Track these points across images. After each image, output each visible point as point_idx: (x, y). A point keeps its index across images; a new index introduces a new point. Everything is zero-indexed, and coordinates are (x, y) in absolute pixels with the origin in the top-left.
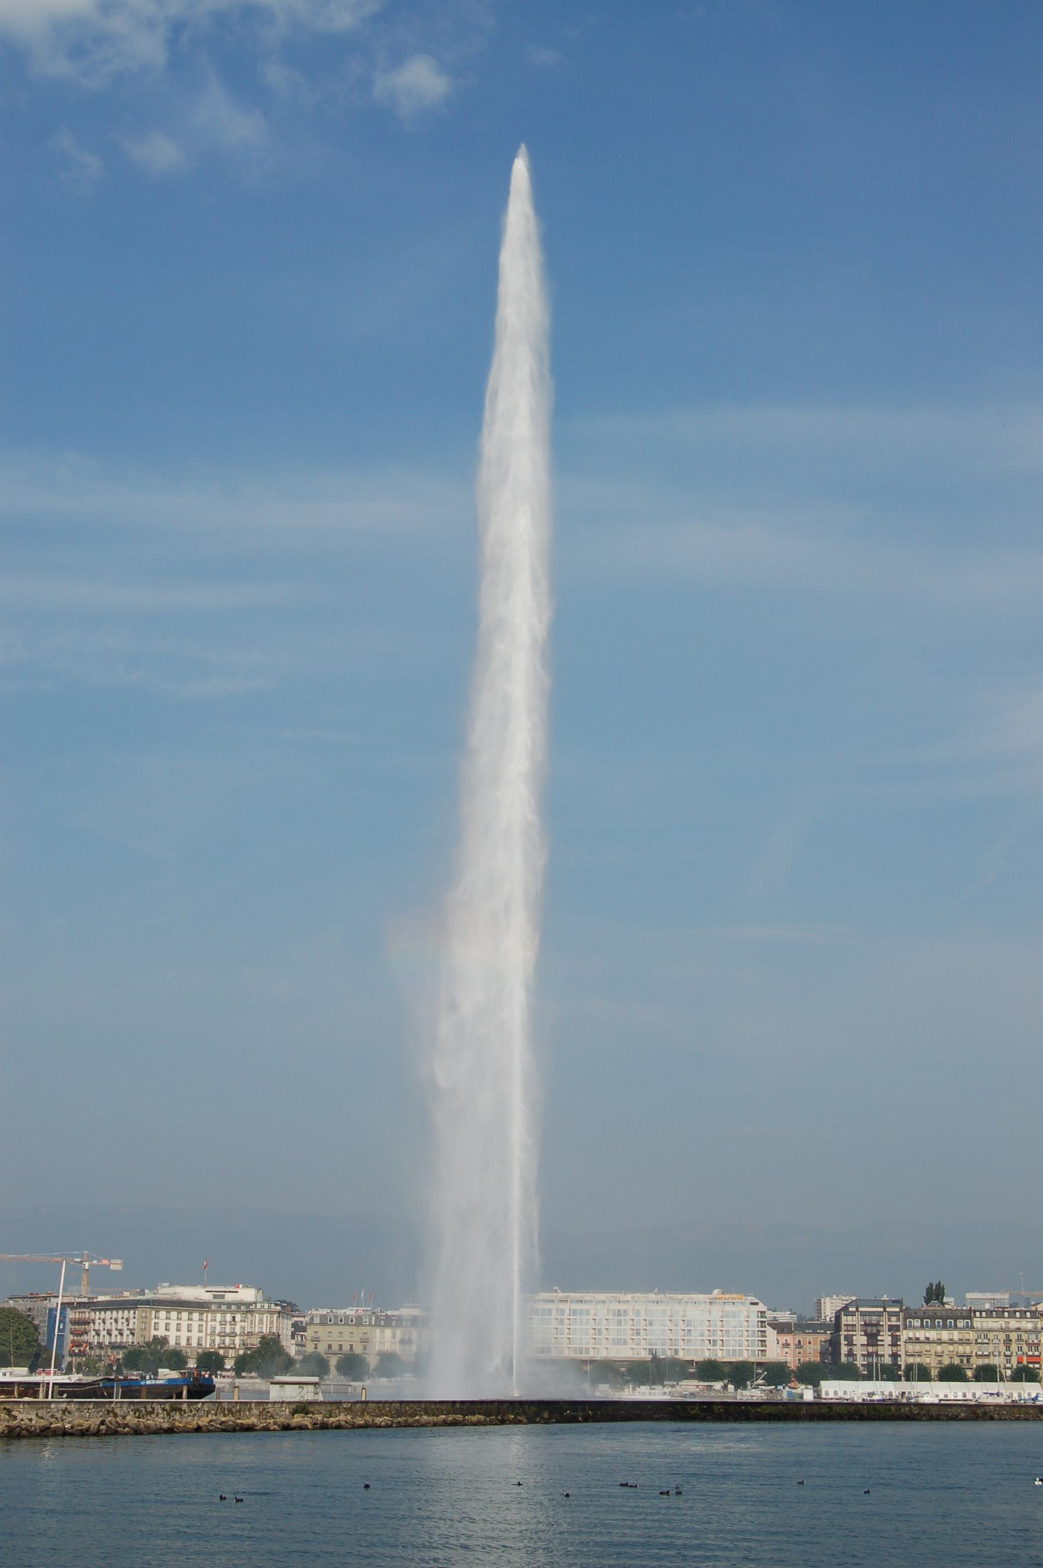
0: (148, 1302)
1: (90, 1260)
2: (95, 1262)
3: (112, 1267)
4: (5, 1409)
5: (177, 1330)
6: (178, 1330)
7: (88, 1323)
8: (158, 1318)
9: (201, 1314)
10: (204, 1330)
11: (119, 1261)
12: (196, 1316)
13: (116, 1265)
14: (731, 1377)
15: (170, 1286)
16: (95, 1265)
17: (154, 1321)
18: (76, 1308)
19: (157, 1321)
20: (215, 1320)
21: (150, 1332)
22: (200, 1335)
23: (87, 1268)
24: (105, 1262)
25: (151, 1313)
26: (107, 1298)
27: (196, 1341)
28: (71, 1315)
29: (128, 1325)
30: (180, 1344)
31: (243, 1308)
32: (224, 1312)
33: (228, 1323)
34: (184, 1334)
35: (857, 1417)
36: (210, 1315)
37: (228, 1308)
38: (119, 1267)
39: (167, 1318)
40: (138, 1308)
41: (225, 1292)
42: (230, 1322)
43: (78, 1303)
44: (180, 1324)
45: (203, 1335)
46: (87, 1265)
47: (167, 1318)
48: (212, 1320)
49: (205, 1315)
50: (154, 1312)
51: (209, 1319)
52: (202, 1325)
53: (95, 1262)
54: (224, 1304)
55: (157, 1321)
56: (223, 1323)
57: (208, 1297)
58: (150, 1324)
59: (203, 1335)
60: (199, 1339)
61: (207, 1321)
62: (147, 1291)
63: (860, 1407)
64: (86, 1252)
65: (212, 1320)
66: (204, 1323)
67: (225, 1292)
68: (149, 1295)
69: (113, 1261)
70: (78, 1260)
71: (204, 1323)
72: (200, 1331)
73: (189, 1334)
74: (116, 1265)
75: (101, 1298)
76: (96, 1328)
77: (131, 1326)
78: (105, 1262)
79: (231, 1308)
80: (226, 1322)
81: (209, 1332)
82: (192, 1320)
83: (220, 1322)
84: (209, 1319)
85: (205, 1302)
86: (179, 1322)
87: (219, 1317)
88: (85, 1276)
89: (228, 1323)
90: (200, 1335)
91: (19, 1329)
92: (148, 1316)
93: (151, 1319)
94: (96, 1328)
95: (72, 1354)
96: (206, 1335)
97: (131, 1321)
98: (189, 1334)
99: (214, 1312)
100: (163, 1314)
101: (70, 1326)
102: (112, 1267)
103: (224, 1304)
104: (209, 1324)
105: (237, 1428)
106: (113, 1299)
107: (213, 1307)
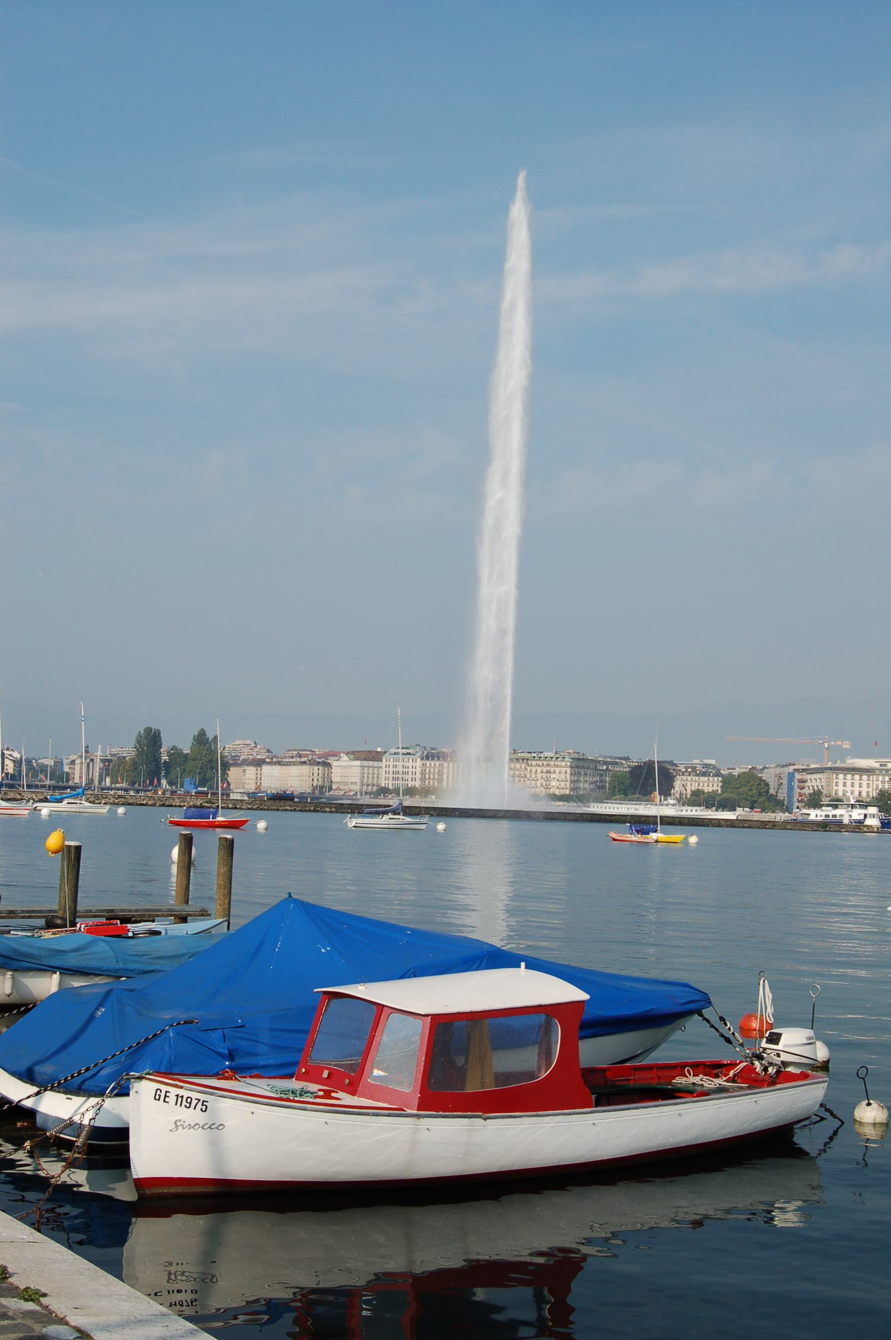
0: (831, 769)
1: (829, 741)
2: (832, 743)
3: (844, 746)
4: (18, 793)
5: (860, 787)
6: (844, 786)
7: (805, 782)
8: (838, 779)
9: (869, 776)
10: (871, 785)
11: (848, 742)
12: (865, 777)
13: (846, 745)
14: (721, 806)
15: (851, 758)
16: (832, 744)
17: (835, 781)
18: (801, 772)
19: (837, 780)
20: (878, 780)
21: (832, 787)
22: (868, 790)
23: (826, 747)
24: (839, 743)
25: (833, 776)
26: (818, 766)
27: (858, 794)
28: (798, 776)
29: (821, 783)
30: (838, 795)
31: (884, 772)
32: (884, 775)
33: (886, 782)
34: (857, 789)
35: (666, 823)
36: (875, 777)
37: (886, 772)
38: (848, 747)
39: (844, 779)
40: (824, 772)
41: (887, 762)
42: (888, 782)
43: (802, 769)
44: (853, 783)
45: (870, 790)
46: (826, 745)
47: (844, 779)
48: (876, 780)
49: (871, 777)
50: (835, 775)
51: (875, 779)
52: (869, 783)
53: (832, 743)
54: (884, 770)
55: (837, 780)
56: (883, 782)
57: (877, 765)
58: (832, 783)
59: (870, 790)
60: (868, 792)
61: (873, 781)
62: (838, 761)
63: (683, 819)
64: (826, 737)
65: (876, 780)
66: (871, 782)
67: (887, 762)
68: (838, 764)
69: (845, 742)
70: (821, 742)
71: (871, 782)
72: (868, 787)
73: (860, 789)
74: (846, 745)
75: (812, 766)
76: (808, 785)
77: (822, 784)
78: (839, 743)
79: (888, 772)
80: (885, 781)
81: (874, 788)
82: (854, 779)
83: (882, 781)
84: (875, 779)
85: (872, 769)
86: (853, 781)
87: (881, 778)
88: (826, 752)
89: (886, 782)
90: (868, 790)
91: (754, 785)
92: (831, 777)
93: (833, 779)
94: (813, 785)
95: (799, 801)
96: (873, 790)
97: (823, 780)
98: (860, 789)
99: (878, 775)
100: (841, 776)
101: (798, 784)
102: (844, 746)
103: (884, 770)
104: (875, 783)
105: (135, 804)
106: (821, 767)
107: (877, 772)
